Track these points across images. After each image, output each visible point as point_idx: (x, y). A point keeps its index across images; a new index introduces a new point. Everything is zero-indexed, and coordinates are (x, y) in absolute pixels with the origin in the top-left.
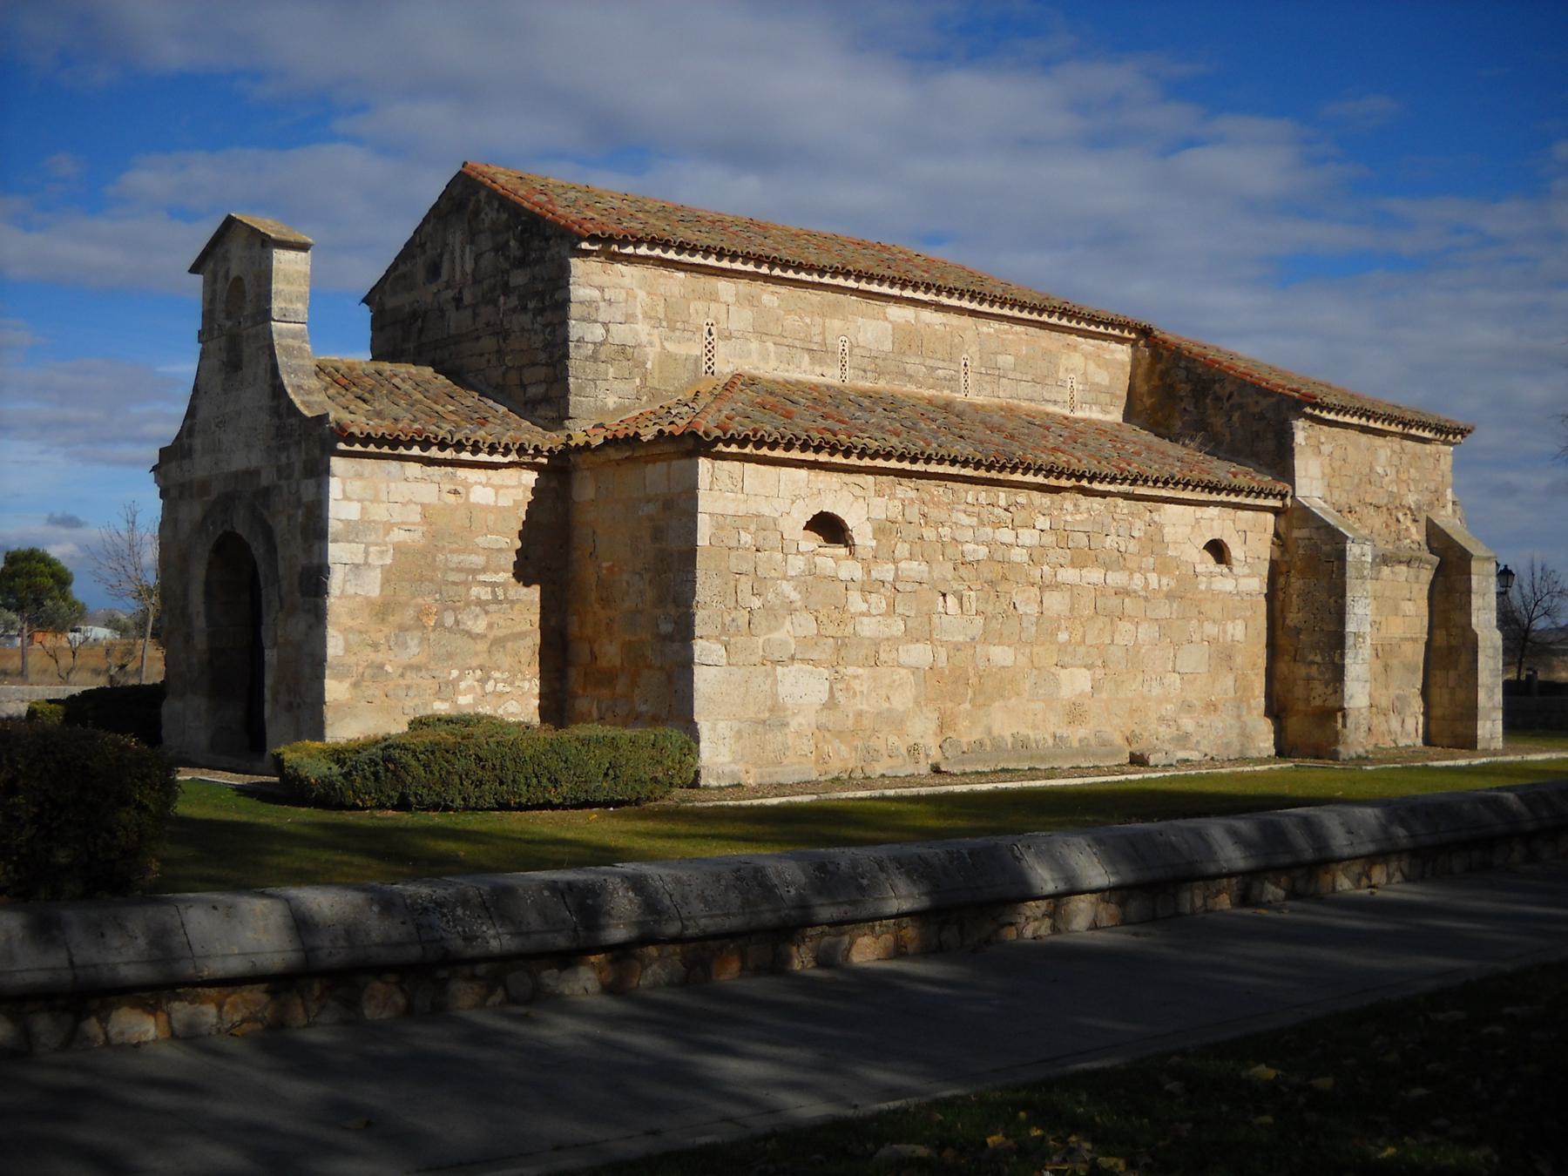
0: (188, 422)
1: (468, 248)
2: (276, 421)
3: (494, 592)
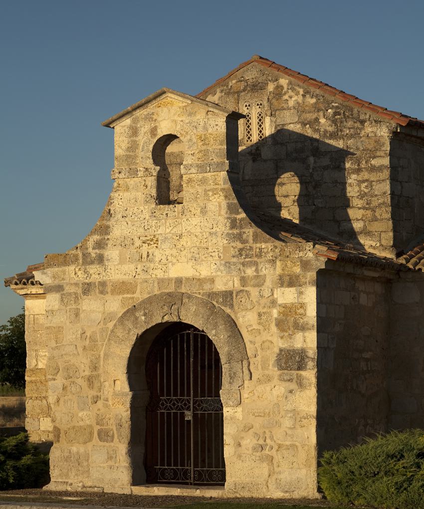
0: (96, 237)
1: (267, 120)
2: (239, 245)
3: (367, 365)
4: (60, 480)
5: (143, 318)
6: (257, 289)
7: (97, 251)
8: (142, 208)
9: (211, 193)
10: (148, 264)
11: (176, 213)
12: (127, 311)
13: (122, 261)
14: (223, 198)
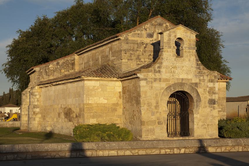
2: (199, 71)
4: (145, 137)
5: (173, 89)
6: (203, 83)
7: (159, 69)
8: (172, 58)
9: (191, 56)
10: (174, 74)
11: (182, 60)
12: (168, 87)
13: (166, 73)
14: (194, 57)
